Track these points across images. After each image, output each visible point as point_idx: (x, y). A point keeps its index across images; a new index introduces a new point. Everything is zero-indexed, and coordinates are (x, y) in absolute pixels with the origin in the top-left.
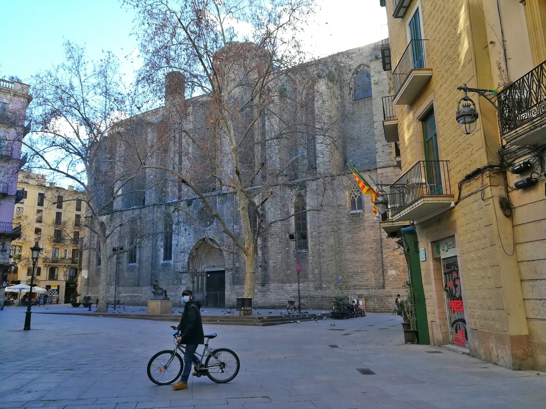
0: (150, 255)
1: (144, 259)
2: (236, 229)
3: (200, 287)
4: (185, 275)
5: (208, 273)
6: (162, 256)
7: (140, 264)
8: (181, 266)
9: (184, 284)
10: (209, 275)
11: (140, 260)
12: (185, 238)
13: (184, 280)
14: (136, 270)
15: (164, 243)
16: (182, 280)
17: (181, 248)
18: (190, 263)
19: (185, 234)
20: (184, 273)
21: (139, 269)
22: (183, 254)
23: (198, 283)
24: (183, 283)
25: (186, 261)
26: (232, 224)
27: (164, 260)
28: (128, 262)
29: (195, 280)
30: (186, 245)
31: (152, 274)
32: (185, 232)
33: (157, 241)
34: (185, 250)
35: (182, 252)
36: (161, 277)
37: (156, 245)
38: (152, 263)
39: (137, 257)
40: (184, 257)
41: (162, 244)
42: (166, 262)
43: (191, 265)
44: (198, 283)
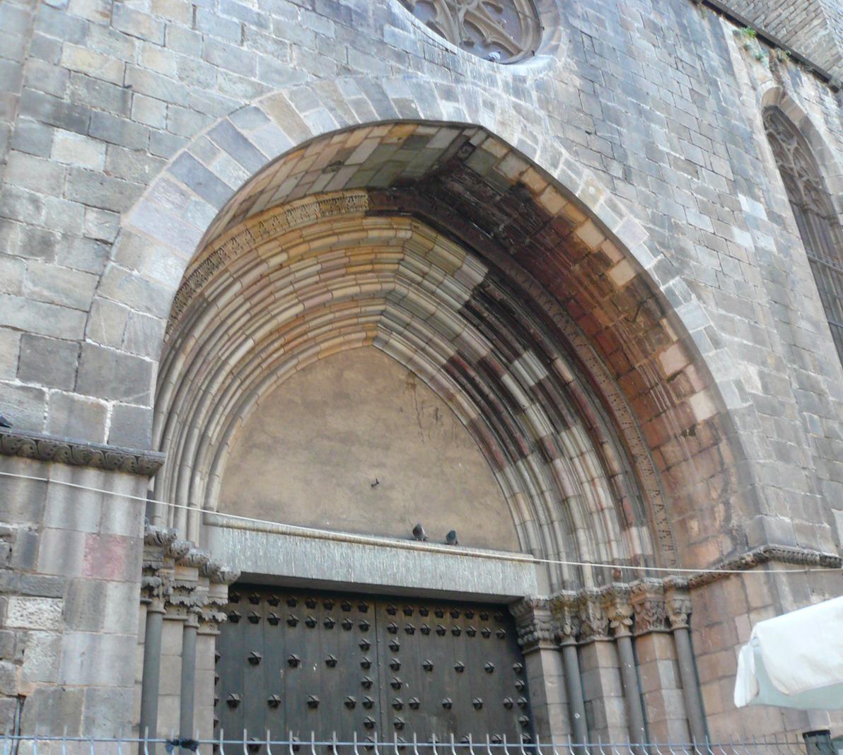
20: (78, 459)
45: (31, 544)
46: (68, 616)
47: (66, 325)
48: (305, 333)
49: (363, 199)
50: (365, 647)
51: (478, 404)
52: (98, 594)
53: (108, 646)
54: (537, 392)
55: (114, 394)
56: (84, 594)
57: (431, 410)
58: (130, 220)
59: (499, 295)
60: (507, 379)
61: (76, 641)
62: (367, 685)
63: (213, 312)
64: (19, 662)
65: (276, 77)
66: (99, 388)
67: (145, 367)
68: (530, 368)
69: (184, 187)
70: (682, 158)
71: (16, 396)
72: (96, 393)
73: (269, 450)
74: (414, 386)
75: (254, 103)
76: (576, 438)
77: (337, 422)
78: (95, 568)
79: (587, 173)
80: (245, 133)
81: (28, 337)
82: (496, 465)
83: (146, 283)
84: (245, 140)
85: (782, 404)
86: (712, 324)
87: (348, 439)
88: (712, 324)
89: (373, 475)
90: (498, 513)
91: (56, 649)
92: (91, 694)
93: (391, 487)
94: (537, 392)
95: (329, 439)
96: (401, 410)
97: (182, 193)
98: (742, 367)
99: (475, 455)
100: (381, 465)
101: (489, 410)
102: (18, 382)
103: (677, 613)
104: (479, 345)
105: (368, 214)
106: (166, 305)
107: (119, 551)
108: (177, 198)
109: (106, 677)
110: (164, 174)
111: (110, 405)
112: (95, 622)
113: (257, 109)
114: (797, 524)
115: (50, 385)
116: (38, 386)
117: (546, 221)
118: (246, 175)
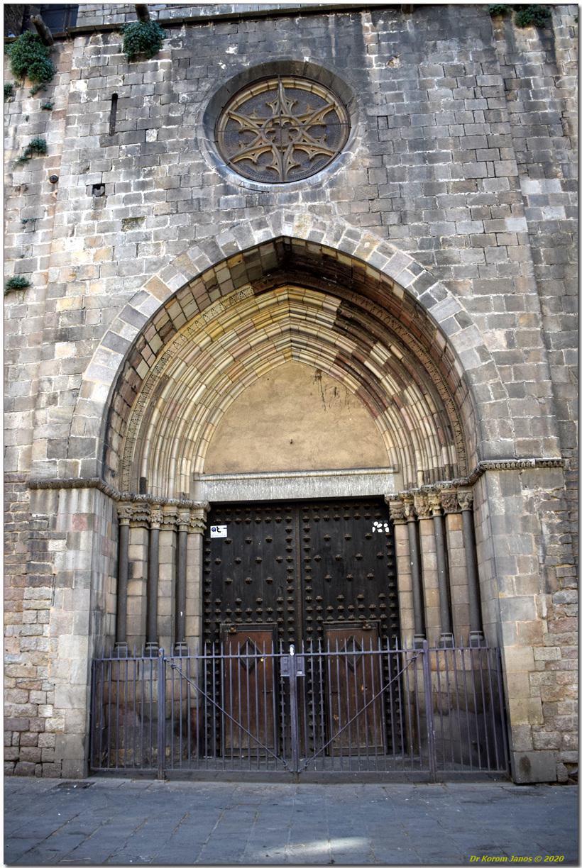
2: (543, 200)
3: (165, 606)
4: (82, 501)
5: (218, 512)
8: (44, 432)
9: (65, 579)
10: (220, 532)
12: (91, 244)
13: (72, 543)
16: (54, 546)
17: (49, 307)
18: (116, 422)
19: (95, 217)
20: (69, 486)
22: (64, 350)
23: (151, 581)
24: (56, 567)
25: (100, 394)
26: (508, 168)
29: (137, 552)
30: (98, 289)
32: (97, 205)
34: (94, 319)
35: (64, 336)
40: (77, 367)
43: (115, 443)
44: (151, 581)
45: (55, 520)
46: (68, 545)
47: (62, 433)
48: (244, 367)
49: (248, 290)
50: (289, 531)
51: (358, 380)
52: (78, 536)
53: (81, 555)
54: (392, 367)
55: (82, 456)
56: (73, 536)
57: (332, 390)
58: (85, 376)
59: (349, 315)
60: (367, 363)
61: (71, 554)
62: (289, 551)
63: (171, 382)
64: (53, 563)
65: (154, 267)
66: (76, 455)
67: (93, 441)
68: (380, 354)
69: (108, 350)
70: (464, 179)
71: (47, 465)
72: (75, 458)
73: (232, 435)
74: (320, 378)
75: (142, 288)
76: (411, 393)
77: (270, 411)
78: (76, 527)
79: (365, 233)
80: (137, 308)
81: (50, 440)
82: (374, 416)
83: (93, 404)
84: (137, 311)
85: (526, 352)
86: (464, 309)
87: (277, 419)
88: (464, 309)
89: (292, 436)
90: (376, 445)
91: (65, 558)
92: (76, 573)
93: (303, 442)
94: (387, 368)
95: (266, 422)
96: (311, 394)
97: (108, 353)
98: (489, 335)
99: (363, 411)
100: (297, 430)
101: (365, 383)
102: (47, 460)
103: (462, 501)
104: (348, 346)
105: (256, 295)
106: (101, 411)
107: (85, 519)
108: (105, 357)
109: (81, 566)
110: (100, 346)
111: (80, 461)
112: (77, 547)
113: (143, 291)
114: (519, 442)
115: (58, 458)
116: (54, 459)
117: (352, 270)
118: (136, 331)
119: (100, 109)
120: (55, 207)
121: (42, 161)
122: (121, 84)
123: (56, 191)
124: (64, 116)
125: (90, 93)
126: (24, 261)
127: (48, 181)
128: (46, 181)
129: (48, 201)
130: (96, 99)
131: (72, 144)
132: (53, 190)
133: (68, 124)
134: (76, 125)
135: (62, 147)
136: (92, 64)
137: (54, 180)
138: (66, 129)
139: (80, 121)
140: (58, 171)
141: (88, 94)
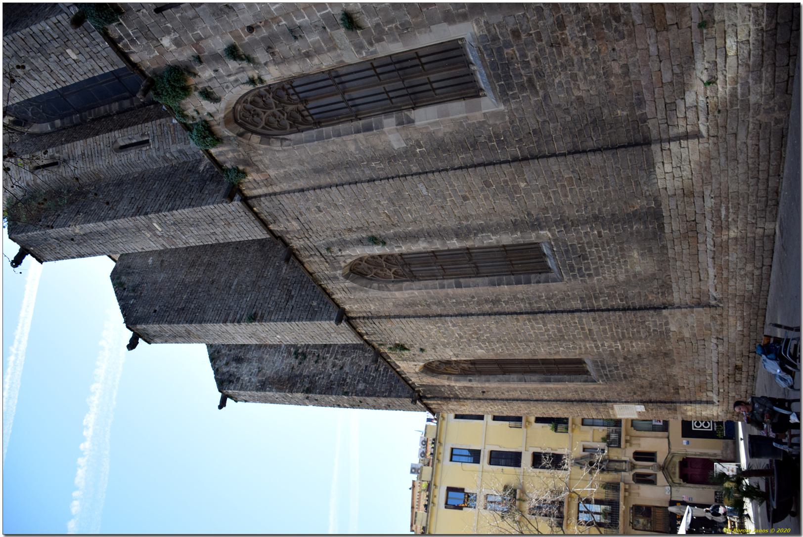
0: (474, 178)
1: (507, 208)
6: (457, 110)
7: (536, 225)
11: (516, 226)
14: (571, 237)
15: (387, 112)
21: (563, 223)
27: (477, 93)
28: (543, 276)
31: (575, 152)
33: (391, 157)
36: (582, 89)
37: (408, 154)
38: (515, 160)
39: (506, 239)
41: (389, 122)
42: (481, 79)
119: (174, 18)
120: (272, 19)
121: (241, 46)
122: (144, 11)
123: (259, 24)
124: (197, 44)
125: (167, 32)
126: (327, 25)
127: (254, 33)
128: (255, 35)
129: (270, 27)
130: (169, 25)
131: (214, 28)
132: (259, 27)
133: (201, 39)
134: (199, 32)
135: (222, 35)
136: (145, 42)
137: (251, 29)
138: (206, 38)
139: (193, 30)
140: (242, 30)
141: (169, 33)
